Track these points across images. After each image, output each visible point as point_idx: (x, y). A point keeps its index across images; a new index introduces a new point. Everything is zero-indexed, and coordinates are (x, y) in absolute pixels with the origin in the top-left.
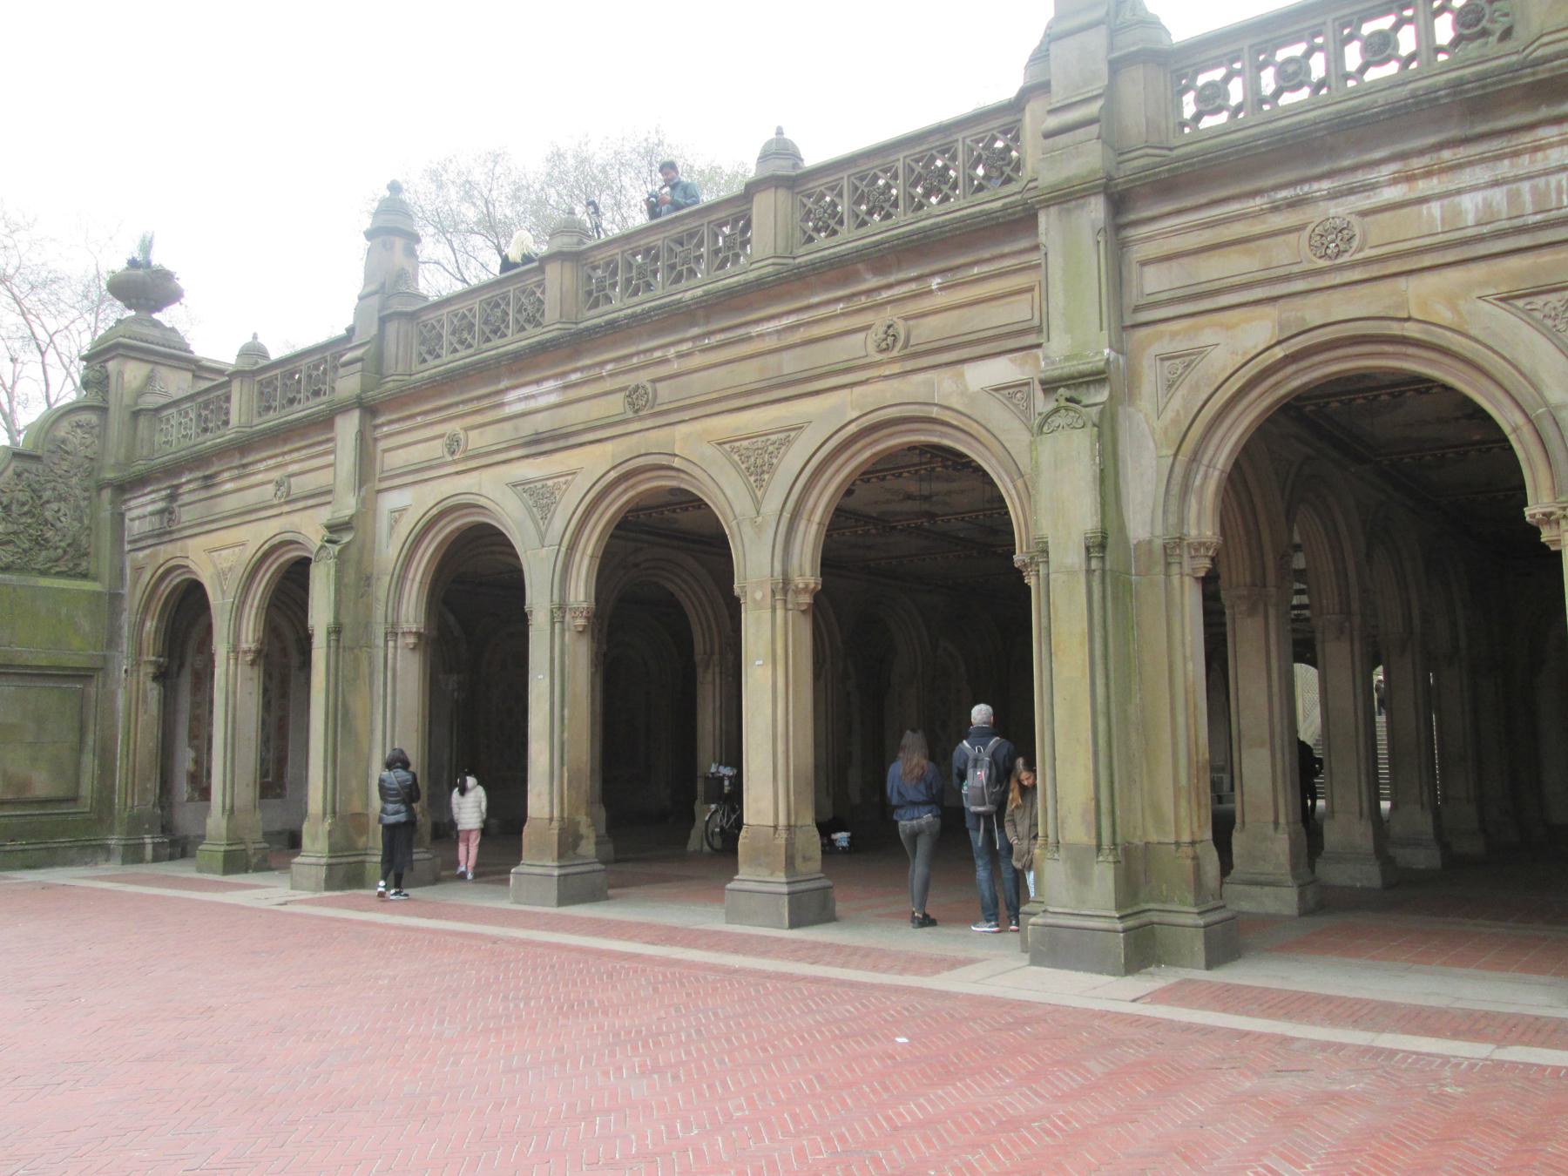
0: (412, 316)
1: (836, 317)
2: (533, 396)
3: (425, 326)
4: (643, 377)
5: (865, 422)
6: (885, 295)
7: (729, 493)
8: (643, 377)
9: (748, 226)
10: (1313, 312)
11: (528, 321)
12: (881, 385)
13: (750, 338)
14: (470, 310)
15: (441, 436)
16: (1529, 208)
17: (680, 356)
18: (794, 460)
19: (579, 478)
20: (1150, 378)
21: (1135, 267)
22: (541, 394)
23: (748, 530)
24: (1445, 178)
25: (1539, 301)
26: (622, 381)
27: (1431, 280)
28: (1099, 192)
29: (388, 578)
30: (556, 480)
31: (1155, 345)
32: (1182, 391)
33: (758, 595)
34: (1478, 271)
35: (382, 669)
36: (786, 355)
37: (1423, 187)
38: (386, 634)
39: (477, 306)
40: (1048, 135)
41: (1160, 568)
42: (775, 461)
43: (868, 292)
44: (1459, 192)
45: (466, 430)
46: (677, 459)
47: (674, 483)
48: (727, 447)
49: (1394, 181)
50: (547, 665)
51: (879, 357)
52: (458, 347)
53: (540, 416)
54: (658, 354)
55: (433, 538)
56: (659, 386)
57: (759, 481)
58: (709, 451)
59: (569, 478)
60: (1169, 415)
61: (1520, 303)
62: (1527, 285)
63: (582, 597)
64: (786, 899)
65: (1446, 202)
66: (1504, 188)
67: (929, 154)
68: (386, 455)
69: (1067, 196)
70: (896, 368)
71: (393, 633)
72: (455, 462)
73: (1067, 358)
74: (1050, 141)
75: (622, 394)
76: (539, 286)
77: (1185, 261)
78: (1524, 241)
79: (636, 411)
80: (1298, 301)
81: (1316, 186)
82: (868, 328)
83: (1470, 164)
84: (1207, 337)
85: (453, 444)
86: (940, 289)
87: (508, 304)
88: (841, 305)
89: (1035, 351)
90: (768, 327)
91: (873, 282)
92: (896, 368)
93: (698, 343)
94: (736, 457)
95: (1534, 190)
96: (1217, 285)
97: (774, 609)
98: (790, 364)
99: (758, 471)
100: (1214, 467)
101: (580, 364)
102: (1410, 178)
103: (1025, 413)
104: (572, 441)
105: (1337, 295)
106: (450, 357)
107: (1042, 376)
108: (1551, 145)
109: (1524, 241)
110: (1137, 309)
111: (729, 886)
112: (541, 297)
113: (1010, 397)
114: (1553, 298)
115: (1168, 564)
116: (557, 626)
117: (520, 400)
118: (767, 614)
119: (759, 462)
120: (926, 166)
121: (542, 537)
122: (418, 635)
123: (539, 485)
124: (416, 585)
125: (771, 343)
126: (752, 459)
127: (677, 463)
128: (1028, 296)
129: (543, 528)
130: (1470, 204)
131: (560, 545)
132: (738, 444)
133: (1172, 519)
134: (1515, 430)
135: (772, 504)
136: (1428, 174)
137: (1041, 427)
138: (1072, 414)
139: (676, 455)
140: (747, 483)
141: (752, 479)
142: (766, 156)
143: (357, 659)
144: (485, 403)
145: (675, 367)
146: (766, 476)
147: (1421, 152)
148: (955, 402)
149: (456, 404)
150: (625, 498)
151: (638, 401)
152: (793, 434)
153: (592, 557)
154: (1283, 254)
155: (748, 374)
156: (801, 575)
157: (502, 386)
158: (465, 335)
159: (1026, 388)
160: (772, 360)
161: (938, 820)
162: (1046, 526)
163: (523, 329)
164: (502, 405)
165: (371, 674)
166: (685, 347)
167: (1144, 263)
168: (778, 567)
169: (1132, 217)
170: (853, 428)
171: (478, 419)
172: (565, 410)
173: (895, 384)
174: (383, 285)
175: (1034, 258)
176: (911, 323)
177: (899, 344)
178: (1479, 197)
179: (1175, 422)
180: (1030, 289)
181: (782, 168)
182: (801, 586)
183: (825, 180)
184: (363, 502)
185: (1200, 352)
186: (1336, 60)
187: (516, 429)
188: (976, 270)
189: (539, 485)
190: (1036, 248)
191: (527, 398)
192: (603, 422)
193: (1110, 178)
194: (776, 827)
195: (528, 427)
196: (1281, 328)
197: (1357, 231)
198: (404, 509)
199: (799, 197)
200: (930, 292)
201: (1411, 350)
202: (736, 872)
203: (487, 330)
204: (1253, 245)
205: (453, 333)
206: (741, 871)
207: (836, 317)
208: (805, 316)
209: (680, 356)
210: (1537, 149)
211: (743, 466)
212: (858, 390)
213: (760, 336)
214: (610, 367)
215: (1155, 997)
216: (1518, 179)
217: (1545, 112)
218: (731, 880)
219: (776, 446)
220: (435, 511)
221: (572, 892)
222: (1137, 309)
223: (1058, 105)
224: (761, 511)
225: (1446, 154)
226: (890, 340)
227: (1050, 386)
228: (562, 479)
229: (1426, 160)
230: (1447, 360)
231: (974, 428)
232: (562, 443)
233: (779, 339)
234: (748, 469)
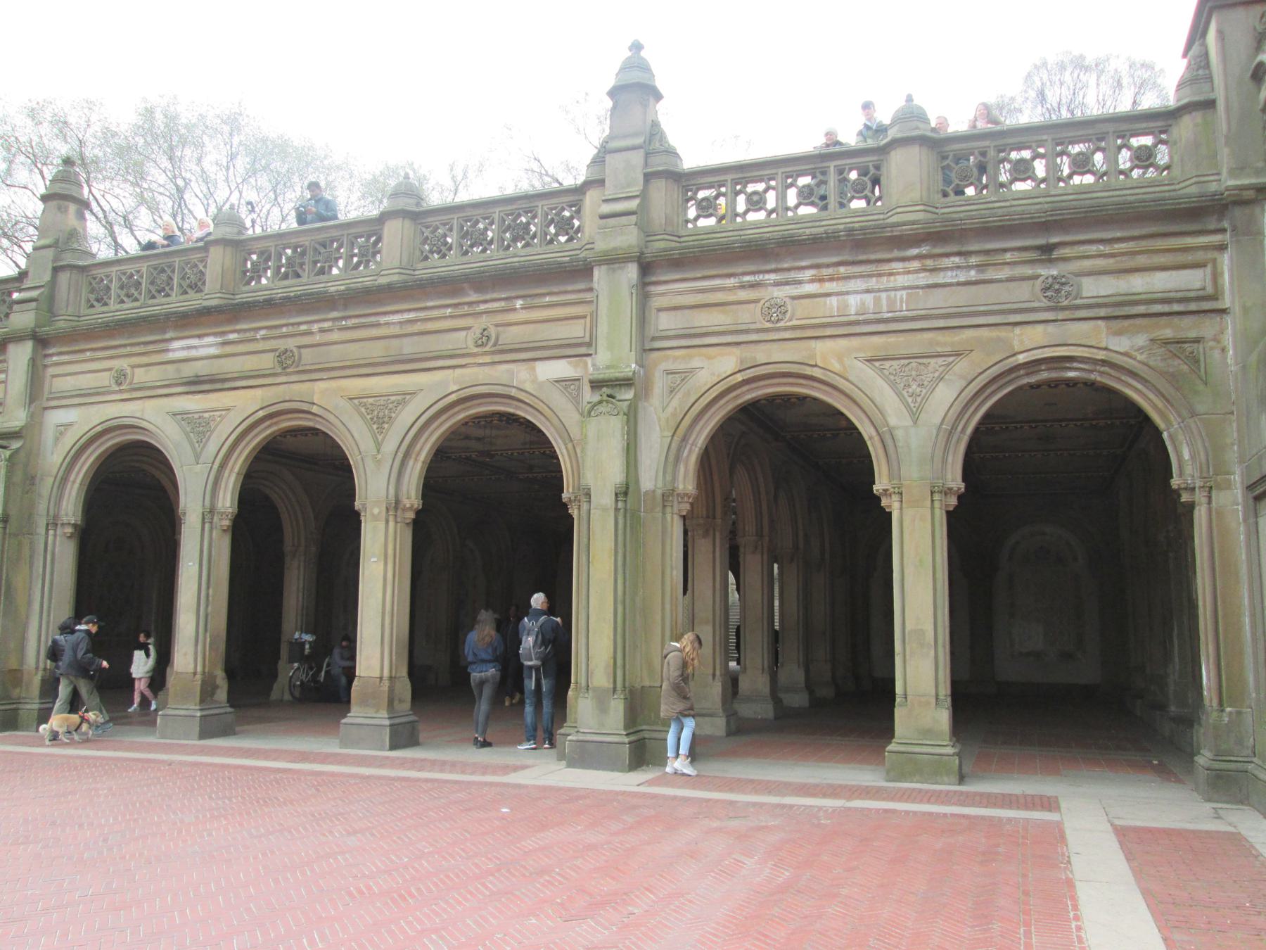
0: (83, 269)
1: (445, 317)
2: (195, 347)
3: (95, 279)
4: (291, 343)
5: (463, 394)
6: (482, 307)
7: (356, 435)
8: (291, 343)
9: (379, 240)
10: (761, 354)
11: (190, 286)
12: (476, 369)
13: (378, 325)
14: (138, 272)
15: (110, 369)
16: (885, 309)
17: (322, 331)
18: (407, 416)
19: (232, 413)
20: (659, 384)
21: (654, 311)
22: (203, 346)
23: (370, 464)
24: (841, 283)
25: (887, 364)
27: (829, 344)
28: (634, 261)
29: (51, 480)
30: (212, 414)
31: (664, 363)
32: (679, 395)
33: (376, 511)
34: (855, 342)
35: (42, 552)
36: (405, 340)
38: (48, 524)
39: (144, 269)
40: (603, 217)
41: (659, 509)
42: (393, 415)
43: (470, 304)
44: (847, 293)
45: (133, 367)
46: (315, 407)
47: (310, 424)
48: (356, 401)
49: (812, 281)
50: (197, 555)
51: (476, 350)
52: (125, 299)
53: (200, 363)
54: (303, 327)
55: (95, 450)
56: (303, 351)
57: (380, 428)
58: (343, 403)
59: (224, 413)
60: (670, 410)
61: (877, 364)
62: (882, 353)
63: (228, 504)
64: (388, 730)
65: (840, 297)
66: (873, 295)
67: (517, 211)
68: (54, 379)
69: (613, 260)
70: (487, 359)
71: (53, 523)
72: (121, 391)
73: (608, 367)
74: (604, 221)
75: (272, 354)
76: (202, 261)
77: (687, 312)
78: (881, 327)
79: (284, 368)
80: (752, 347)
81: (767, 276)
82: (469, 328)
83: (854, 277)
84: (696, 363)
85: (120, 377)
86: (522, 308)
87: (173, 271)
88: (449, 310)
89: (585, 358)
90: (394, 318)
91: (474, 297)
92: (487, 359)
93: (337, 323)
94: (363, 410)
95: (888, 298)
96: (704, 330)
97: (387, 522)
98: (409, 347)
99: (379, 419)
100: (696, 446)
101: (238, 327)
102: (821, 280)
103: (576, 399)
104: (227, 385)
105: (775, 345)
106: (118, 307)
107: (591, 377)
108: (899, 274)
109: (881, 327)
110: (654, 339)
111: (343, 721)
112: (203, 270)
113: (566, 388)
114: (895, 363)
115: (664, 506)
116: (207, 526)
117: (183, 349)
118: (382, 525)
119: (381, 414)
120: (514, 220)
121: (197, 457)
122: (75, 526)
123: (196, 416)
124: (77, 486)
125: (395, 330)
126: (375, 413)
127: (315, 409)
128: (582, 321)
129: (199, 450)
130: (853, 301)
131: (213, 463)
132: (365, 400)
133: (669, 478)
134: (871, 438)
135: (390, 445)
136: (831, 279)
137: (589, 412)
138: (610, 405)
139: (314, 404)
140: (371, 430)
141: (375, 426)
142: (396, 194)
143: (20, 544)
144: (151, 348)
145: (317, 338)
146: (386, 426)
147: (828, 266)
148: (528, 387)
149: (125, 346)
150: (268, 432)
151: (286, 361)
152: (408, 397)
153: (238, 474)
154: (747, 316)
155: (376, 351)
156: (408, 498)
157: (168, 336)
158: (133, 291)
159: (577, 383)
160: (395, 342)
161: (499, 673)
162: (589, 478)
163: (185, 293)
164: (168, 350)
165: (31, 557)
166: (326, 325)
167: (659, 310)
168: (392, 491)
169: (654, 279)
170: (453, 397)
171: (145, 360)
172: (223, 361)
173: (487, 369)
174: (57, 241)
175: (588, 296)
176: (500, 329)
177: (491, 343)
178: (858, 297)
179: (674, 415)
180: (585, 317)
181: (406, 204)
182: (408, 506)
183: (440, 218)
184: (32, 416)
185: (692, 371)
186: (782, 197)
187: (178, 371)
188: (547, 299)
189: (196, 416)
190: (591, 290)
191: (189, 348)
192: (257, 373)
193: (642, 253)
194: (381, 678)
195: (189, 371)
196: (742, 362)
197: (789, 308)
198: (71, 425)
199: (420, 227)
200: (515, 309)
201: (816, 384)
202: (349, 710)
203: (153, 289)
204: (728, 308)
205: (122, 288)
206: (352, 711)
207: (445, 317)
208: (422, 315)
209: (322, 331)
210: (891, 274)
211: (369, 417)
212: (458, 371)
213: (387, 324)
214: (263, 332)
215: (650, 783)
216: (879, 290)
217: (896, 253)
218: (345, 716)
219: (395, 404)
220: (99, 429)
221: (210, 728)
222: (654, 339)
223: (610, 197)
224: (381, 450)
225: (842, 269)
226: (484, 339)
227: (596, 385)
228: (218, 413)
229: (830, 271)
230: (835, 393)
231: (540, 406)
232: (218, 386)
233: (401, 328)
234: (372, 419)
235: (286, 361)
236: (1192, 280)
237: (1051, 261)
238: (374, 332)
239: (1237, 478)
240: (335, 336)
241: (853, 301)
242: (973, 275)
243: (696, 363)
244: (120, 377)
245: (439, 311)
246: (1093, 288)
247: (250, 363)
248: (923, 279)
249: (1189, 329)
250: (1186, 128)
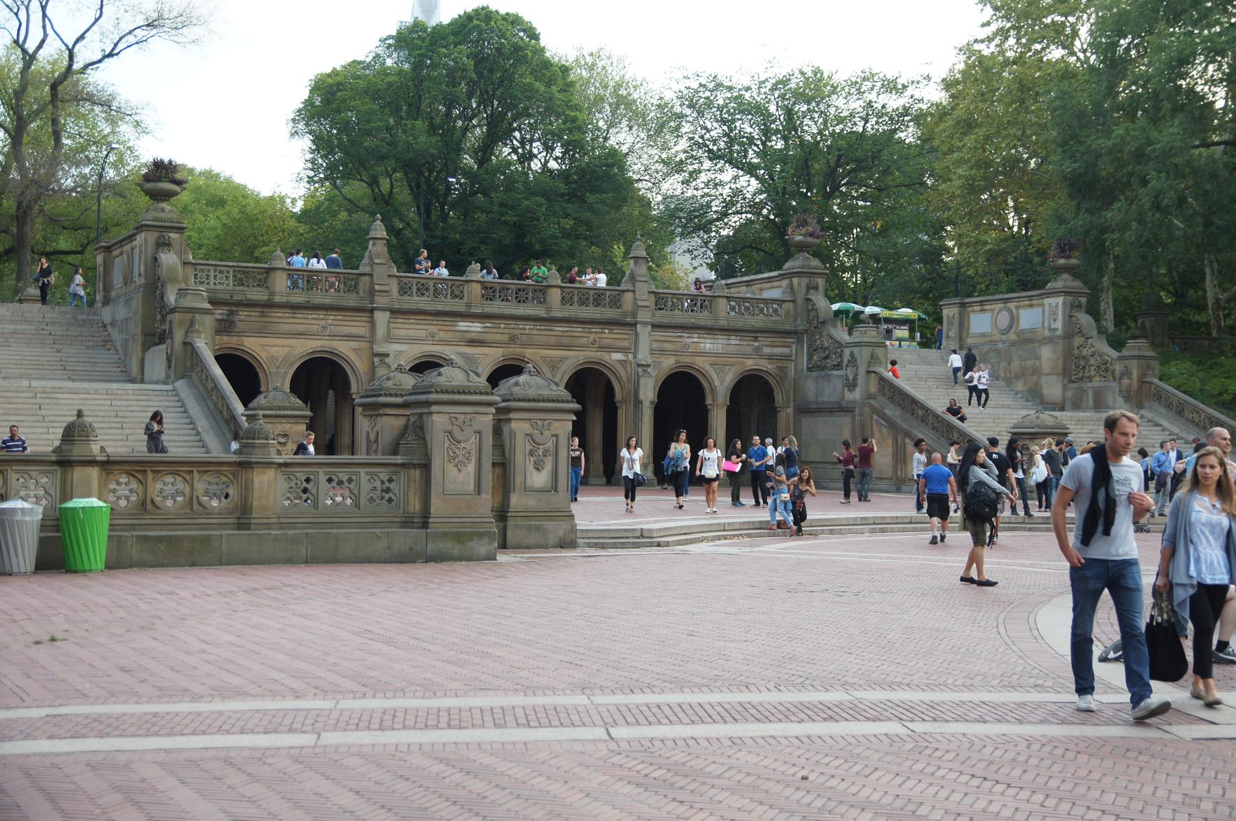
4: (517, 332)
26: (507, 331)
37: (701, 340)
84: (662, 360)
90: (560, 329)
98: (565, 341)
125: (560, 334)
130: (708, 345)
145: (527, 332)
151: (513, 339)
154: (678, 346)
155: (552, 340)
195: (468, 336)
235: (513, 339)
236: (786, 351)
237: (756, 341)
238: (551, 333)
239: (792, 405)
240: (535, 332)
241: (708, 345)
242: (738, 342)
243: (662, 360)
244: (433, 335)
245: (577, 329)
246: (767, 350)
247: (498, 337)
248: (726, 342)
249: (785, 364)
250: (787, 306)
